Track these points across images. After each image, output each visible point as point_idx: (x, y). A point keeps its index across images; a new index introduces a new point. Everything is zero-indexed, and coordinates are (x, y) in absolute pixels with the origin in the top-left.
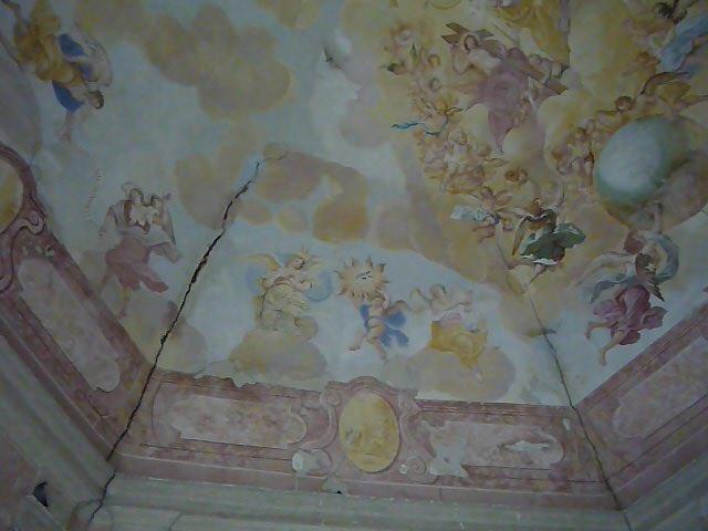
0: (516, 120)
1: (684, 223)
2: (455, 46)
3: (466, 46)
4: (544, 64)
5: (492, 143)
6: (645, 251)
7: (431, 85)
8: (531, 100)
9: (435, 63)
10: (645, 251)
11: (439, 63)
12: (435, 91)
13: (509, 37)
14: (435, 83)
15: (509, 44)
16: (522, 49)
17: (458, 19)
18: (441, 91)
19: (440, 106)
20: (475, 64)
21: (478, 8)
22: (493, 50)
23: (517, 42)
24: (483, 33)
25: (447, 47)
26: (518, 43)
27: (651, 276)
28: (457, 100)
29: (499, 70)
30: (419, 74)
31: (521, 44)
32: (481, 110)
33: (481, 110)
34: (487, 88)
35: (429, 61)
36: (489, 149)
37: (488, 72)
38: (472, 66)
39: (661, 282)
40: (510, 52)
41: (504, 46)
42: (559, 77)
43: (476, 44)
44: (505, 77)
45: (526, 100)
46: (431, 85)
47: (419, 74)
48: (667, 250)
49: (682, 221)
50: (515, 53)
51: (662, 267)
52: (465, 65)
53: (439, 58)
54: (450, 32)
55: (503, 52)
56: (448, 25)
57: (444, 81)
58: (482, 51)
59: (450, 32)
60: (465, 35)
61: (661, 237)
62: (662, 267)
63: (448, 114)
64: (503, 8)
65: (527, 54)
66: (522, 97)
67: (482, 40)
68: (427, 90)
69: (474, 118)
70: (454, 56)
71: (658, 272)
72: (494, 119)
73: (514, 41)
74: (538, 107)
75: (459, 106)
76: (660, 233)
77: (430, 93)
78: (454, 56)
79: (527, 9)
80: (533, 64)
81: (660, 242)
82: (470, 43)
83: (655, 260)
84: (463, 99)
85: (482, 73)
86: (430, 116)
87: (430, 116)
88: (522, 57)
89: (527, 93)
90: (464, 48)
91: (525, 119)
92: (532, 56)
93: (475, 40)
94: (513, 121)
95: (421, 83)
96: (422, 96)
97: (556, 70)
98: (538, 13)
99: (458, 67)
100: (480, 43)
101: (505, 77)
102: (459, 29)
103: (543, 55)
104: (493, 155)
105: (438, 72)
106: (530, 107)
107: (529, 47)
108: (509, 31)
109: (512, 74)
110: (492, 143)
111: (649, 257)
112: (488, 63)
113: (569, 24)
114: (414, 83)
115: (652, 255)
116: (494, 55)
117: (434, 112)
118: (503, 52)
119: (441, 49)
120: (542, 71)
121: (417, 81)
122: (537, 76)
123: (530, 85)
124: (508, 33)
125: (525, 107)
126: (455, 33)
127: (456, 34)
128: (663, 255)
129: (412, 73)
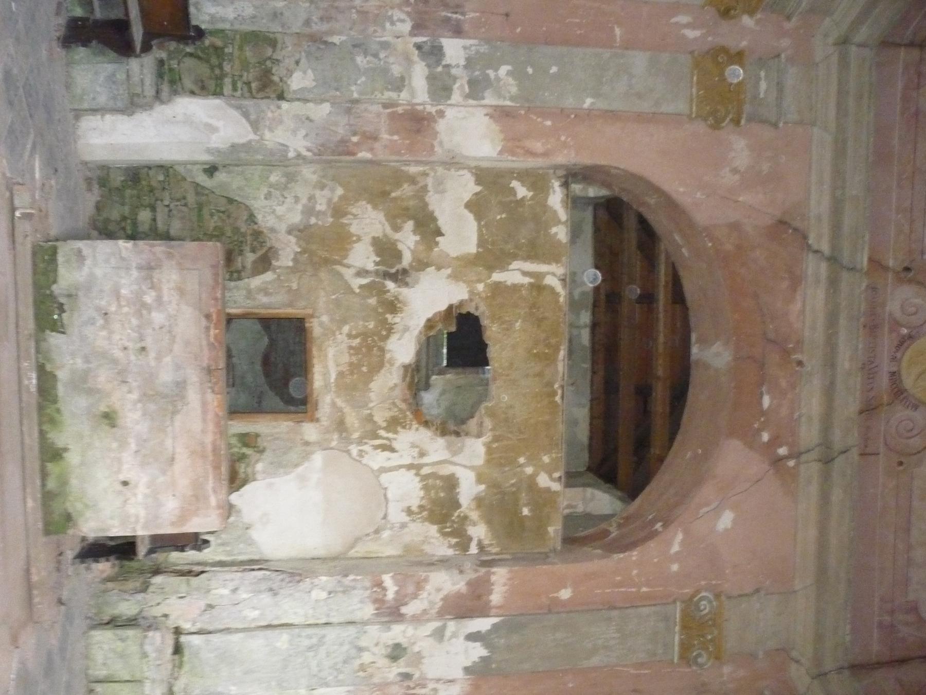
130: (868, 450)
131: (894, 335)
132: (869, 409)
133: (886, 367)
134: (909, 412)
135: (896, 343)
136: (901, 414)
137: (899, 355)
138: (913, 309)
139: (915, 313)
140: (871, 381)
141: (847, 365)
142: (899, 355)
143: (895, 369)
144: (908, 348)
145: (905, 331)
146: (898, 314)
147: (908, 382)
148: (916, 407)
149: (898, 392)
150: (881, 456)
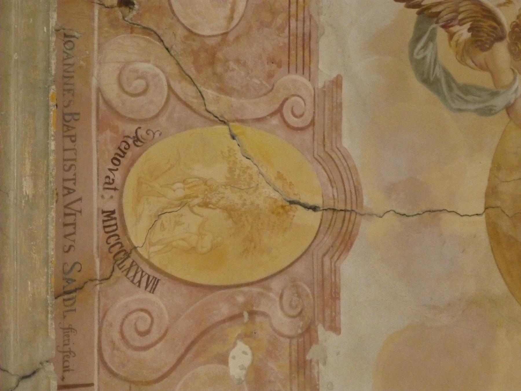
1: (487, 162)
6: (501, 51)
10: (501, 51)
27: (446, 16)
39: (418, 24)
48: (466, 89)
49: (497, 166)
51: (443, 49)
61: (500, 102)
62: (443, 49)
71: (441, 34)
76: (509, 108)
81: (494, 94)
83: (464, 53)
111: (483, 49)
115: (481, 57)
128: (465, 74)
130: (68, 382)
131: (108, 134)
132: (69, 290)
133: (97, 201)
134: (142, 294)
135: (112, 150)
136: (126, 298)
137: (118, 176)
138: (139, 84)
139: (145, 92)
140: (70, 229)
141: (28, 188)
142: (118, 176)
143: (111, 206)
144: (133, 162)
145: (130, 129)
146: (112, 92)
147: (137, 234)
148: (152, 285)
149: (121, 253)
150: (96, 387)
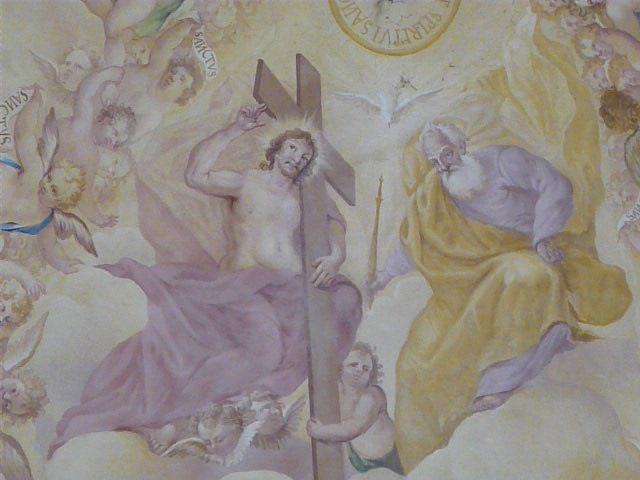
0: (168, 430)
2: (254, 116)
3: (277, 146)
4: (366, 401)
5: (54, 410)
7: (106, 115)
8: (250, 431)
9: (176, 88)
11: (181, 101)
12: (101, 142)
13: (374, 253)
14: (121, 124)
15: (356, 268)
16: (369, 313)
17: (334, 73)
18: (107, 158)
19: (65, 180)
20: (242, 208)
21: (396, 116)
22: (313, 230)
23: (375, 286)
24: (342, 175)
25: (242, 95)
26: (372, 293)
28: (112, 221)
29: (270, 286)
30: (119, 56)
31: (380, 300)
32: (130, 310)
33: (130, 310)
34: (197, 280)
35: (173, 66)
36: (32, 410)
37: (245, 259)
38: (232, 200)
40: (339, 282)
41: (343, 259)
42: (363, 466)
43: (297, 175)
44: (265, 318)
45: (239, 420)
46: (106, 115)
47: (119, 56)
50: (344, 301)
52: (225, 179)
53: (192, 91)
54: (286, 76)
55: (327, 262)
56: (299, 56)
57: (137, 149)
58: (289, 204)
59: (286, 76)
60: (305, 126)
63: (55, 221)
64: (442, 189)
65: (363, 334)
66: (241, 402)
67: (319, 184)
68: (89, 111)
69: (93, 306)
70: (225, 131)
72: (129, 363)
73: (373, 276)
74: (248, 465)
75: (99, 237)
77: (84, 126)
78: (225, 131)
79: (473, 252)
80: (348, 370)
82: (293, 152)
84: (124, 237)
85: (232, 245)
86: (20, 169)
87: (20, 169)
88: (346, 328)
89: (256, 406)
90: (266, 141)
91: (182, 452)
92: (365, 349)
93: (309, 163)
94: (158, 425)
95: (92, 89)
96: (63, 111)
97: (370, 445)
98: (478, 294)
99: (206, 160)
100: (307, 179)
101: (265, 318)
102: (308, 96)
103: (388, 382)
104: (26, 433)
105: (155, 115)
106: (225, 446)
107: (384, 326)
108: (388, 245)
109: (285, 331)
110: (54, 410)
112: (270, 244)
113: (505, 394)
114: (80, 57)
116: (300, 240)
117: (36, 169)
118: (327, 262)
119: (228, 77)
120: (345, 405)
121: (96, 67)
122: (325, 405)
123: (287, 403)
124: (383, 250)
125: (220, 429)
126: (292, 91)
127: (290, 99)
129: (110, 38)
